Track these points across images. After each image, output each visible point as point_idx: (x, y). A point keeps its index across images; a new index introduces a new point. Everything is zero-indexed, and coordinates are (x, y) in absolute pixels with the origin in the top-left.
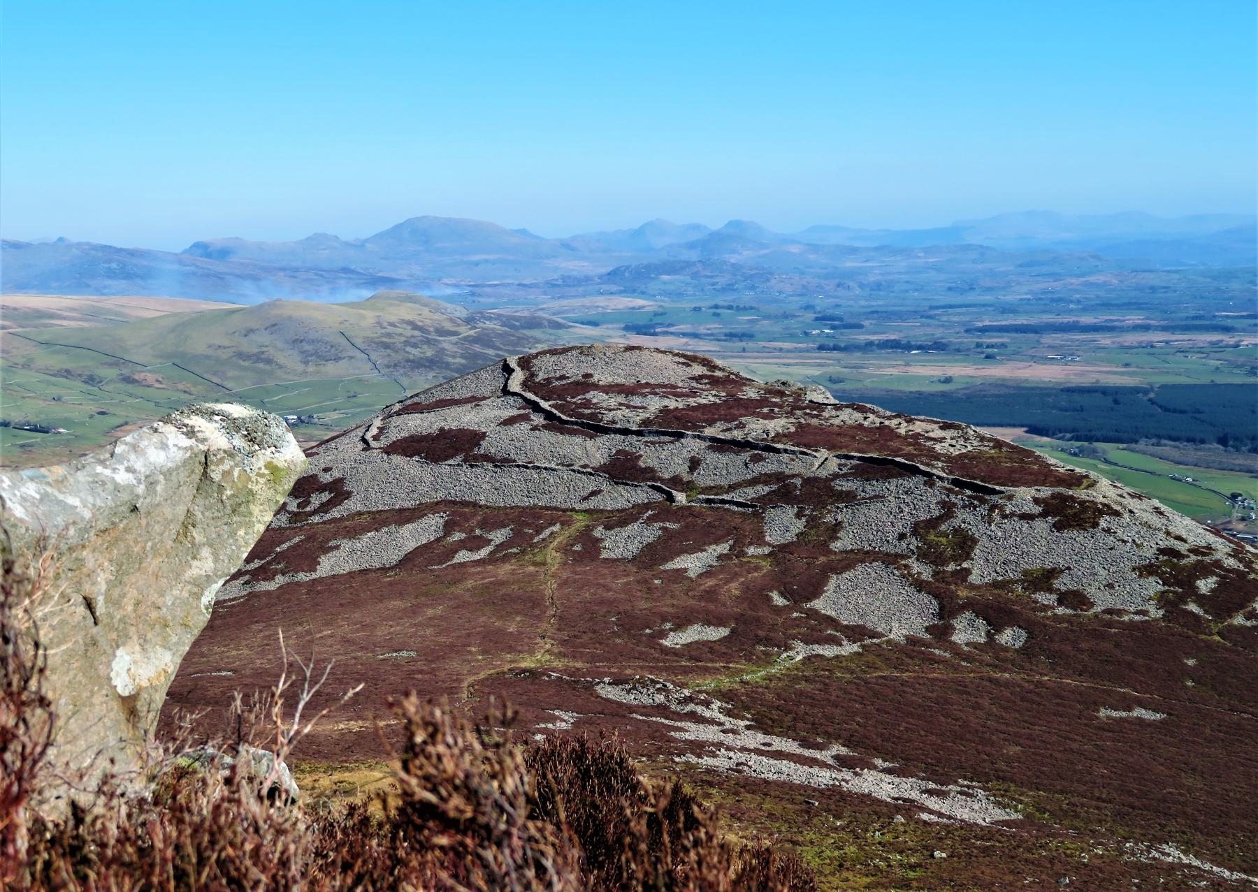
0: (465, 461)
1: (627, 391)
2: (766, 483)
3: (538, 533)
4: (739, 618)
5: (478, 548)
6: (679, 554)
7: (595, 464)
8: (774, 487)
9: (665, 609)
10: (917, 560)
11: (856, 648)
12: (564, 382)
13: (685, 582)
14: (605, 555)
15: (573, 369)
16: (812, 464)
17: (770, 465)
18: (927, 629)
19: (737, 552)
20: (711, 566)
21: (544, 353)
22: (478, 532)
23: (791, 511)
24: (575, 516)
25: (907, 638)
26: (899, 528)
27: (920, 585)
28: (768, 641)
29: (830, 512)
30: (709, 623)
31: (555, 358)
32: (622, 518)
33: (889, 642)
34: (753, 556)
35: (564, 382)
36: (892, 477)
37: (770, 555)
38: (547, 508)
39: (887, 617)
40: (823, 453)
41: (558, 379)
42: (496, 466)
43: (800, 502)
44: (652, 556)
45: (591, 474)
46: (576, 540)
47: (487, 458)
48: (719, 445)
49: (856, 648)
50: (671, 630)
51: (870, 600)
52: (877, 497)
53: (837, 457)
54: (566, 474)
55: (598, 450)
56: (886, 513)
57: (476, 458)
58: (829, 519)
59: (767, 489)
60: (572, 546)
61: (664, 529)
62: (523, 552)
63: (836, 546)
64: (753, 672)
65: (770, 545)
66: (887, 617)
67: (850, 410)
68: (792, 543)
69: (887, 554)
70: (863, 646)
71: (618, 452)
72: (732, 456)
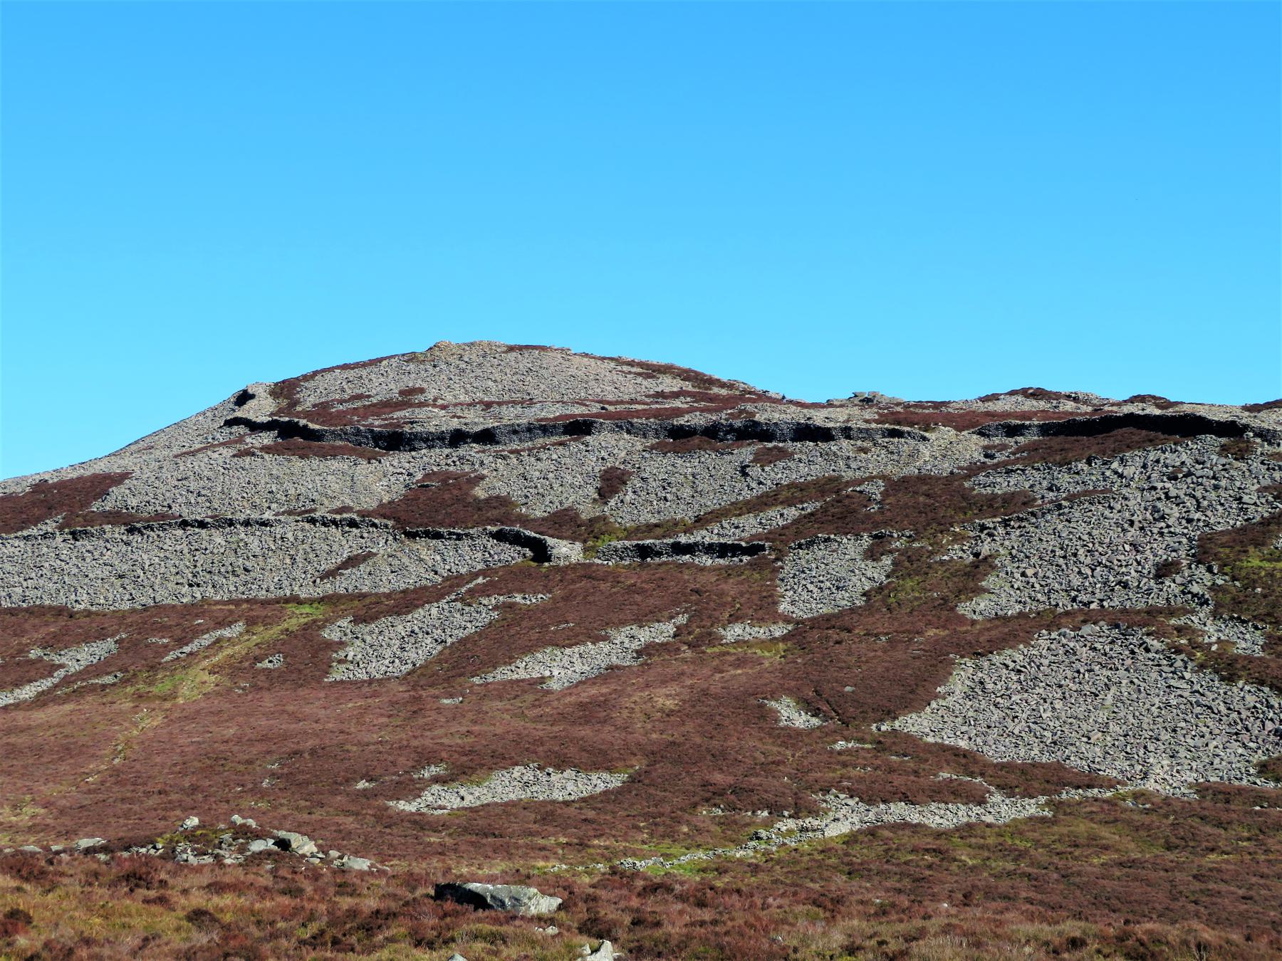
0: (61, 528)
1: (488, 405)
2: (789, 503)
3: (182, 642)
4: (654, 755)
5: (18, 684)
6: (529, 649)
7: (370, 503)
8: (810, 507)
9: (445, 741)
10: (1216, 615)
11: (1032, 808)
12: (358, 404)
13: (530, 698)
14: (339, 673)
15: (382, 387)
16: (914, 454)
17: (807, 464)
18: (1263, 768)
19: (698, 638)
20: (611, 668)
21: (331, 370)
22: (34, 653)
23: (852, 547)
24: (291, 607)
25: (1202, 789)
26: (1158, 551)
27: (1228, 668)
28: (739, 797)
29: (958, 538)
30: (561, 764)
31: (351, 374)
32: (406, 602)
33: (1137, 796)
34: (738, 643)
35: (358, 404)
36: (1129, 447)
37: (784, 638)
38: (230, 602)
39: (1133, 744)
40: (948, 433)
41: (341, 402)
42: (131, 531)
43: (876, 525)
44: (460, 661)
45: (353, 524)
46: (272, 648)
47: (114, 517)
48: (679, 437)
49: (1032, 808)
50: (436, 780)
51: (1080, 711)
52: (1086, 493)
53: (981, 434)
54: (290, 529)
55: (383, 479)
56: (1123, 524)
57: (91, 520)
58: (958, 553)
59: (792, 513)
60: (258, 659)
61: (512, 606)
62: (125, 682)
63: (978, 608)
64: (667, 856)
65: (787, 620)
66: (1133, 744)
67: (1020, 398)
68: (852, 610)
69: (1124, 611)
70: (1057, 806)
71: (426, 476)
72: (709, 458)
